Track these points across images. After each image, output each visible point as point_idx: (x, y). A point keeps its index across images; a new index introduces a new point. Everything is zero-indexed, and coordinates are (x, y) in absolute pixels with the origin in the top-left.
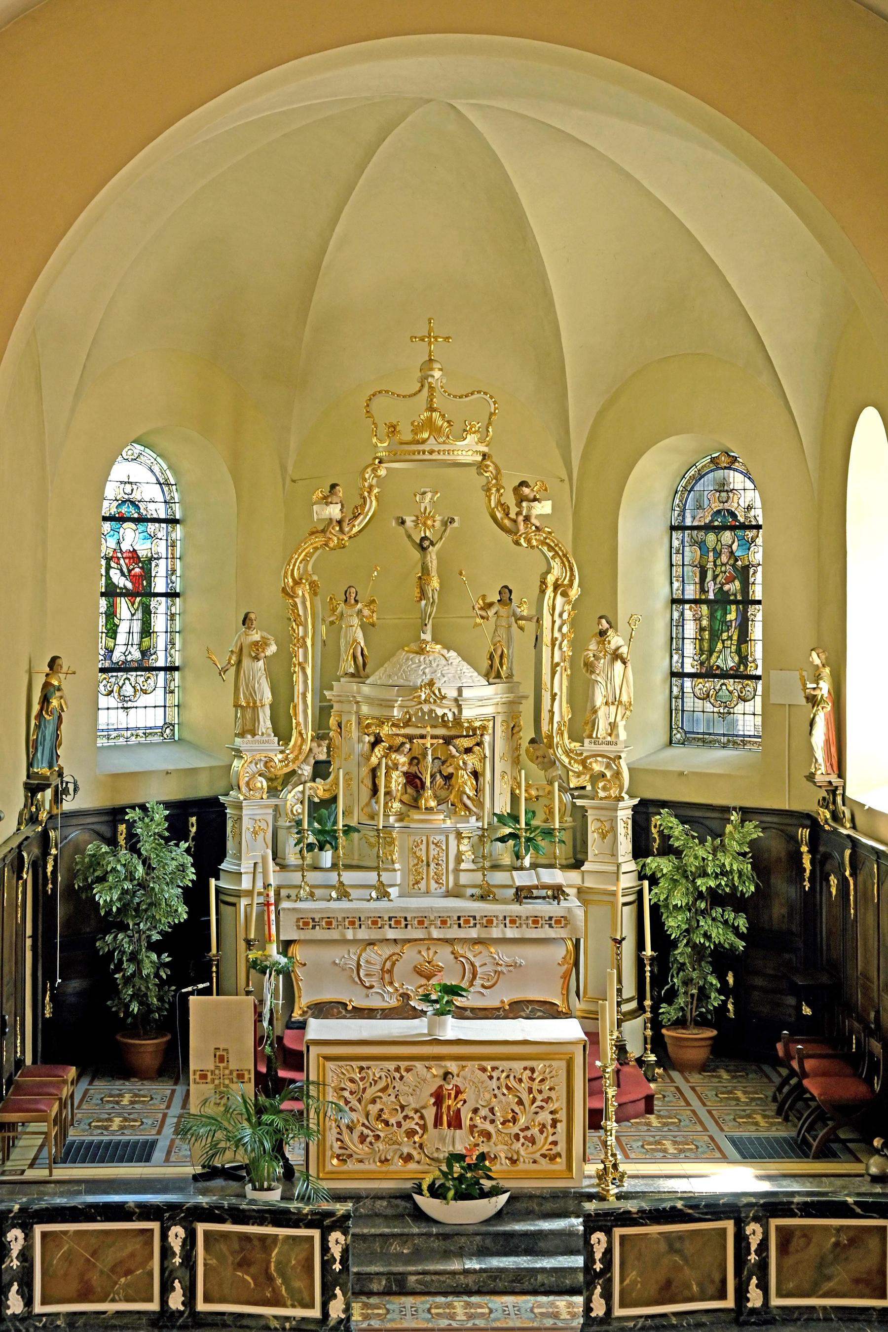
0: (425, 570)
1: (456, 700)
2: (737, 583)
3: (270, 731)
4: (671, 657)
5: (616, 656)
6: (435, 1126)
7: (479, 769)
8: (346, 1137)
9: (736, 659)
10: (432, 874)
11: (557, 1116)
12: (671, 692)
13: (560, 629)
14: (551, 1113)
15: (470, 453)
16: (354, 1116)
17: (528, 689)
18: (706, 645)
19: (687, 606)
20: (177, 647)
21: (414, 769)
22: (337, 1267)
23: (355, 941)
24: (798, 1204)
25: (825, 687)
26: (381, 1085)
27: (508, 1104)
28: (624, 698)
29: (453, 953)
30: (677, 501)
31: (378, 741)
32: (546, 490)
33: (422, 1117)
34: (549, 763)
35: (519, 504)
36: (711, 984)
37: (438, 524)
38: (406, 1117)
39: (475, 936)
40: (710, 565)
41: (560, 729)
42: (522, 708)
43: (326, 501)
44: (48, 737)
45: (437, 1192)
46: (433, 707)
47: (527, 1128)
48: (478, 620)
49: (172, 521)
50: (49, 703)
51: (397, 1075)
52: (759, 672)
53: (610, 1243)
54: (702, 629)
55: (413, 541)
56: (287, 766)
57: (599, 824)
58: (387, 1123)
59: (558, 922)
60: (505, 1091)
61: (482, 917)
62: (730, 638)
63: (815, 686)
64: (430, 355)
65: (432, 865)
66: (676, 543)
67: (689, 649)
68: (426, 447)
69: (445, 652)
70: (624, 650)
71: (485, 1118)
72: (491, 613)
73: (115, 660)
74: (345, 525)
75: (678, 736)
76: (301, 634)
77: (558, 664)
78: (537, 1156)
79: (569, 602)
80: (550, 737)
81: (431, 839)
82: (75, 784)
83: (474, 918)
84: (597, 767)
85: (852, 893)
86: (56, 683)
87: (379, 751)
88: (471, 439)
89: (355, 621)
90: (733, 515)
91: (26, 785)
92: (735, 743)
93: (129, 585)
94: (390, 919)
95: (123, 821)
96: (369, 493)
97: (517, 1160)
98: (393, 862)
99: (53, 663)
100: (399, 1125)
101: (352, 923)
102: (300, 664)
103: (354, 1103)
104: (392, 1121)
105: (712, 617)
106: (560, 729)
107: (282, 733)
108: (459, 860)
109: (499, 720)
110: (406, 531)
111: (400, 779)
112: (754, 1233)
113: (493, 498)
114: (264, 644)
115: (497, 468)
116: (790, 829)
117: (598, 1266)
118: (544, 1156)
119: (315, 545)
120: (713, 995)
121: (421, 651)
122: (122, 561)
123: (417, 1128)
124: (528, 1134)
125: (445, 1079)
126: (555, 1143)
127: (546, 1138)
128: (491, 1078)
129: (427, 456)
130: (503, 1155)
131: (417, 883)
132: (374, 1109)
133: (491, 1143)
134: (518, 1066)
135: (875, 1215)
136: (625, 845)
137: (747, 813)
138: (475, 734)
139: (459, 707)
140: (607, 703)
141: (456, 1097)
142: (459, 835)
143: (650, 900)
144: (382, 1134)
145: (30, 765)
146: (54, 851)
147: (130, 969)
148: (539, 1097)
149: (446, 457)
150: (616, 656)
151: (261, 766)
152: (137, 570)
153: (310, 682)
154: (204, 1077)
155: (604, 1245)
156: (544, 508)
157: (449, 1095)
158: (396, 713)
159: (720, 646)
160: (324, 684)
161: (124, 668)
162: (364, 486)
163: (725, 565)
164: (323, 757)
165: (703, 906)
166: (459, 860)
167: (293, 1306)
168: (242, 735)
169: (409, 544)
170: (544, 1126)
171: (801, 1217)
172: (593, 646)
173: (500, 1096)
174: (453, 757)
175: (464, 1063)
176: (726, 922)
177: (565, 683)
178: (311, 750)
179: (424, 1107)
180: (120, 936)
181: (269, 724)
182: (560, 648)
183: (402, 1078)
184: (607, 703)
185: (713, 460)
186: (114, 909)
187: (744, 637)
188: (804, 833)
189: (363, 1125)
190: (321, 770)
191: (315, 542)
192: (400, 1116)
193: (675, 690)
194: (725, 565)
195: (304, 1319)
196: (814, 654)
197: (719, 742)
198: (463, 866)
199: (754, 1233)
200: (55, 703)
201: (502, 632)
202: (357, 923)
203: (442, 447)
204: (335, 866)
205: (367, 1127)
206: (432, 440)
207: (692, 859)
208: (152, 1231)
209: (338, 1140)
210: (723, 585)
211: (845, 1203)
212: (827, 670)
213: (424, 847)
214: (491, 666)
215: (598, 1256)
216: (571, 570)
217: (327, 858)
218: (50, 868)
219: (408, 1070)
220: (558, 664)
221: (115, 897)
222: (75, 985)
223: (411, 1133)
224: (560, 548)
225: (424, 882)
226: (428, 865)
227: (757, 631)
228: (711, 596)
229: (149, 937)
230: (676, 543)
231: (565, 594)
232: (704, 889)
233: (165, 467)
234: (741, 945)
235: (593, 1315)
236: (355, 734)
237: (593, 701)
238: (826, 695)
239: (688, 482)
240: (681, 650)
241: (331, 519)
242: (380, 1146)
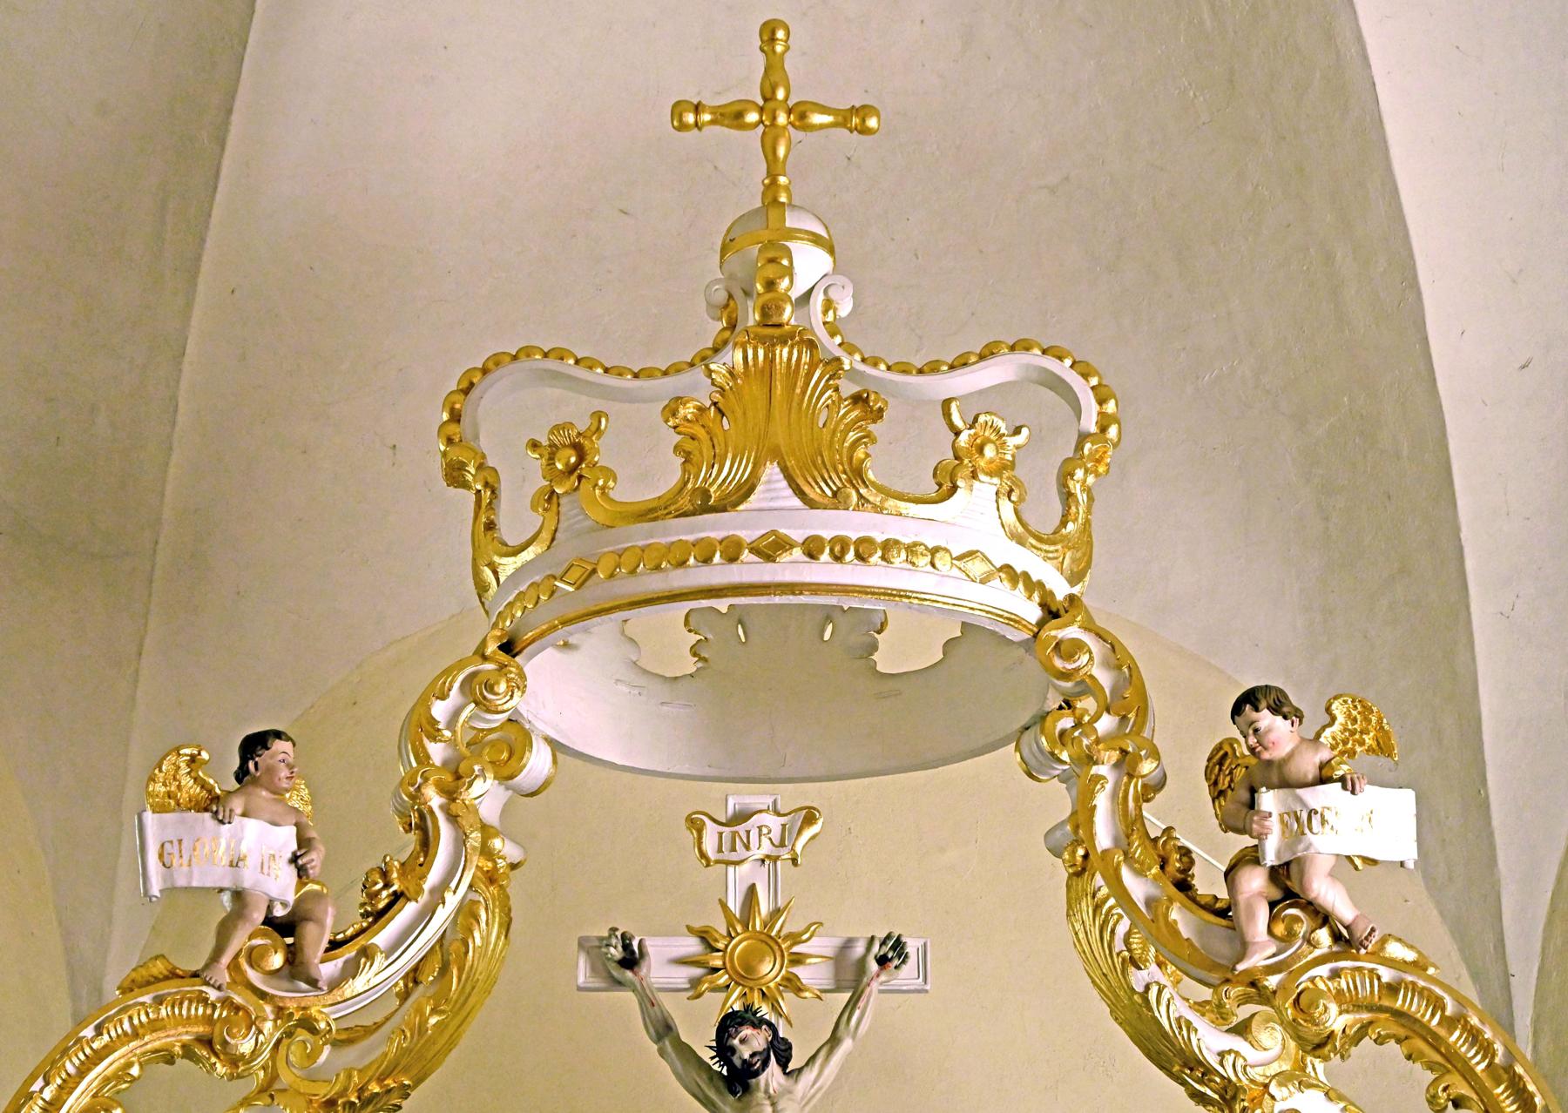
15: (977, 568)
64: (772, 186)
74: (315, 938)
110: (648, 1002)
113: (1102, 801)
115: (1116, 655)
119: (154, 1041)
129: (750, 570)
149: (850, 573)
162: (423, 758)
191: (155, 1026)
206: (773, 488)
224: (1474, 1036)
241: (239, 895)
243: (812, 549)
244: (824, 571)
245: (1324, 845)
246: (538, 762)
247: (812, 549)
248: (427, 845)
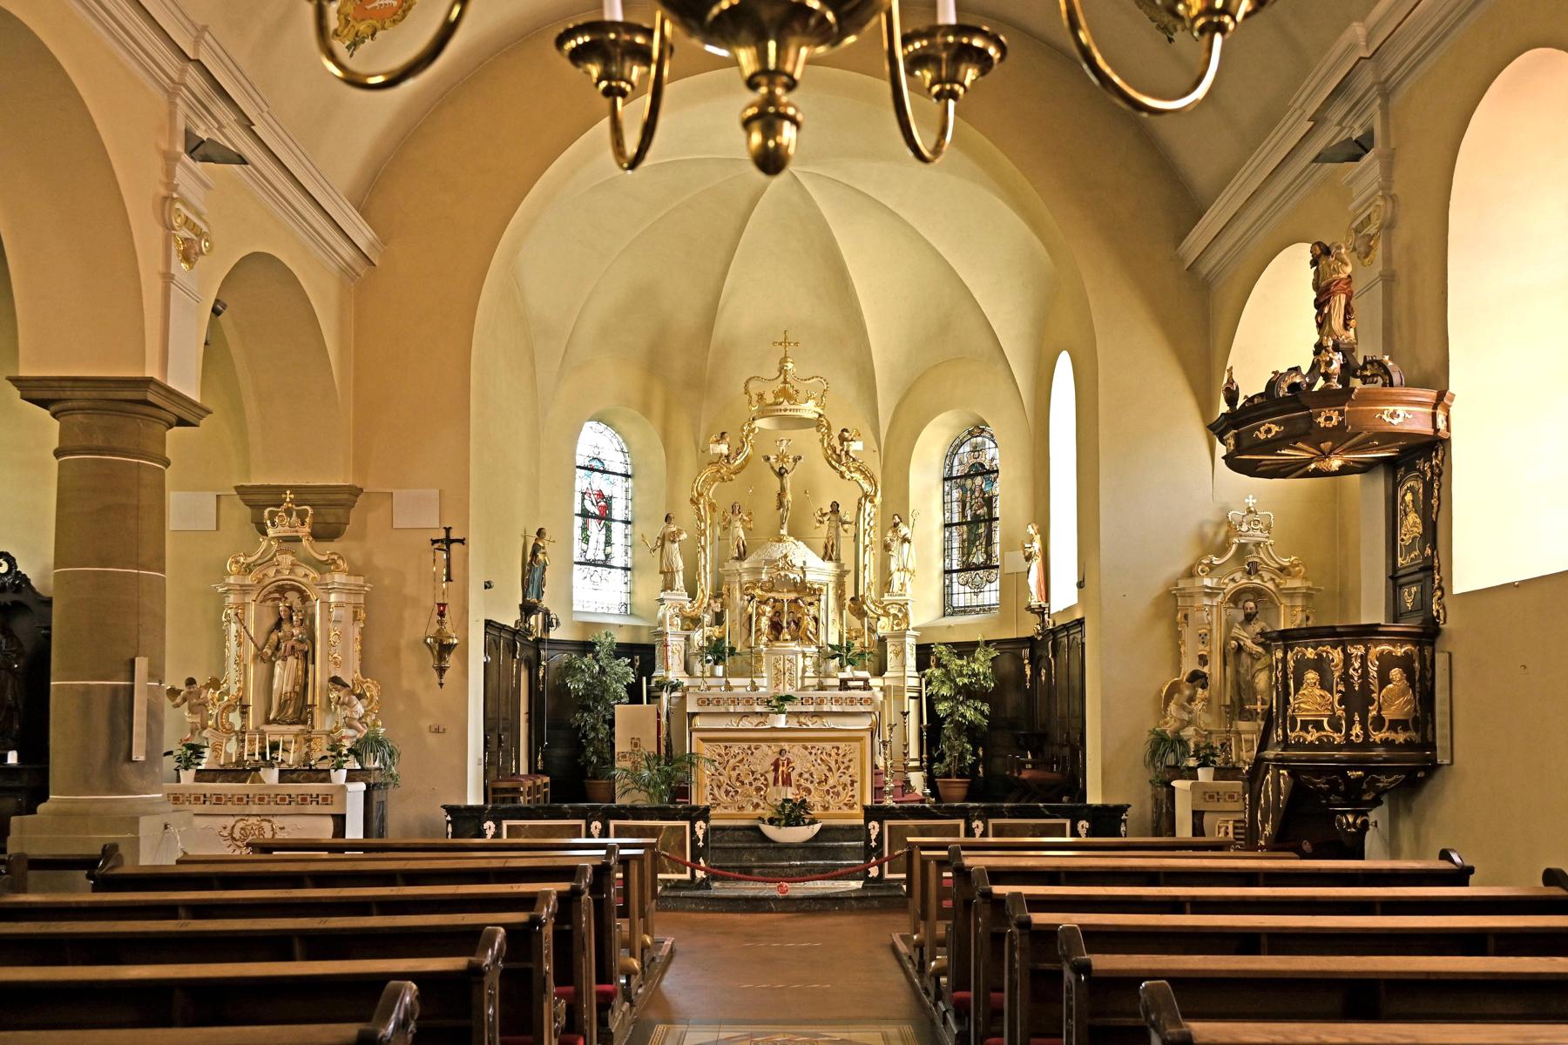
0: (783, 489)
1: (802, 568)
2: (985, 508)
3: (683, 589)
4: (944, 561)
5: (905, 540)
6: (774, 785)
7: (817, 616)
8: (716, 791)
9: (985, 557)
10: (787, 679)
11: (855, 779)
12: (944, 583)
13: (868, 524)
14: (850, 776)
16: (721, 778)
17: (849, 566)
18: (966, 550)
19: (954, 528)
20: (629, 555)
21: (776, 619)
22: (701, 844)
23: (735, 714)
24: (1007, 807)
25: (1037, 545)
26: (738, 758)
27: (822, 770)
28: (910, 567)
29: (798, 722)
30: (947, 462)
31: (753, 597)
32: (859, 435)
33: (766, 779)
34: (860, 613)
35: (842, 444)
36: (967, 750)
37: (791, 460)
38: (755, 779)
39: (813, 710)
40: (968, 499)
41: (869, 587)
42: (845, 579)
43: (718, 442)
44: (536, 578)
45: (771, 821)
46: (787, 573)
47: (835, 787)
48: (818, 525)
49: (627, 476)
50: (537, 556)
51: (750, 752)
52: (998, 564)
53: (881, 828)
54: (963, 541)
55: (774, 471)
56: (694, 611)
57: (894, 647)
58: (743, 783)
59: (866, 701)
60: (819, 761)
61: (817, 698)
62: (981, 544)
63: (1030, 546)
65: (787, 674)
66: (947, 489)
67: (956, 554)
68: (782, 407)
69: (795, 542)
70: (908, 536)
71: (807, 780)
72: (826, 518)
73: (588, 558)
74: (731, 458)
75: (949, 610)
76: (703, 528)
77: (867, 546)
78: (841, 805)
79: (875, 506)
80: (863, 596)
81: (786, 657)
82: (557, 620)
83: (812, 699)
84: (892, 611)
85: (1053, 668)
86: (541, 545)
87: (754, 604)
88: (811, 403)
89: (738, 524)
90: (982, 465)
91: (522, 607)
92: (984, 610)
93: (598, 513)
94: (758, 699)
95: (592, 652)
96: (746, 439)
97: (828, 807)
98: (762, 672)
99: (540, 533)
100: (751, 784)
101: (733, 702)
102: (702, 547)
103: (721, 769)
104: (746, 781)
105: (970, 531)
106: (869, 587)
107: (692, 595)
108: (804, 671)
109: (831, 586)
110: (771, 464)
111: (767, 622)
112: (978, 827)
113: (825, 441)
114: (680, 532)
116: (1017, 651)
117: (873, 844)
118: (846, 805)
120: (968, 757)
121: (780, 540)
122: (592, 496)
123: (762, 786)
124: (836, 790)
125: (780, 754)
126: (853, 796)
127: (847, 793)
128: (811, 753)
129: (783, 413)
130: (819, 805)
131: (777, 685)
132: (734, 774)
133: (811, 796)
134: (828, 746)
135: (1058, 815)
136: (911, 661)
137: (987, 643)
138: (815, 594)
139: (804, 572)
140: (898, 570)
141: (788, 765)
142: (804, 656)
143: (926, 694)
144: (740, 790)
145: (524, 597)
146: (543, 663)
147: (592, 735)
148: (842, 766)
149: (795, 413)
150: (905, 540)
151: (677, 610)
152: (603, 504)
153: (708, 558)
154: (624, 757)
155: (877, 830)
156: (856, 447)
157: (783, 763)
158: (764, 577)
159: (975, 550)
160: (719, 562)
161: (593, 563)
163: (977, 498)
164: (718, 610)
165: (961, 699)
166: (804, 671)
167: (673, 873)
168: (664, 590)
169: (772, 473)
170: (846, 785)
171: (1009, 818)
172: (890, 534)
173: (816, 765)
174: (801, 607)
175: (793, 744)
176: (976, 709)
177: (872, 559)
178: (709, 605)
179: (767, 772)
180: (585, 715)
181: (682, 584)
182: (869, 535)
183: (752, 753)
184: (898, 570)
185: (969, 433)
186: (580, 694)
187: (989, 542)
188: (1026, 652)
189: (727, 784)
190: (719, 619)
192: (751, 778)
193: (947, 582)
194: (977, 498)
195: (679, 880)
196: (1030, 527)
197: (975, 611)
198: (807, 674)
199: (978, 827)
200: (540, 557)
201: (833, 531)
202: (736, 702)
203: (792, 407)
204: (724, 675)
205: (730, 786)
206: (786, 403)
207: (953, 666)
208: (580, 826)
209: (711, 794)
210: (976, 511)
211: (1038, 807)
212: (1038, 536)
213: (781, 662)
214: (826, 553)
215: (873, 837)
216: (876, 486)
217: (719, 670)
218: (541, 675)
219: (756, 749)
220: (867, 546)
221: (581, 687)
222: (558, 752)
223: (758, 789)
225: (781, 685)
226: (784, 674)
227: (997, 538)
228: (969, 519)
229: (604, 716)
230: (947, 489)
231: (872, 501)
232: (961, 684)
233: (621, 440)
234: (985, 722)
235: (870, 876)
236: (738, 595)
237: (890, 568)
238: (1037, 551)
239: (954, 449)
240: (950, 556)
242: (738, 798)
243: (790, 410)
244: (792, 413)
245: (851, 449)
246: (757, 430)
247: (790, 410)
248: (744, 446)
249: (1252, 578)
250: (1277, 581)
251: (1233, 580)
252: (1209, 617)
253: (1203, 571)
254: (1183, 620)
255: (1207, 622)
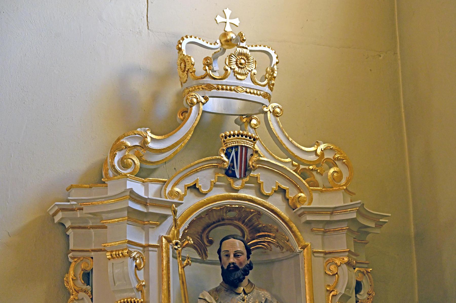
249: (237, 184)
250: (292, 194)
251: (194, 187)
252: (141, 274)
253: (125, 166)
254: (80, 283)
255: (136, 285)
